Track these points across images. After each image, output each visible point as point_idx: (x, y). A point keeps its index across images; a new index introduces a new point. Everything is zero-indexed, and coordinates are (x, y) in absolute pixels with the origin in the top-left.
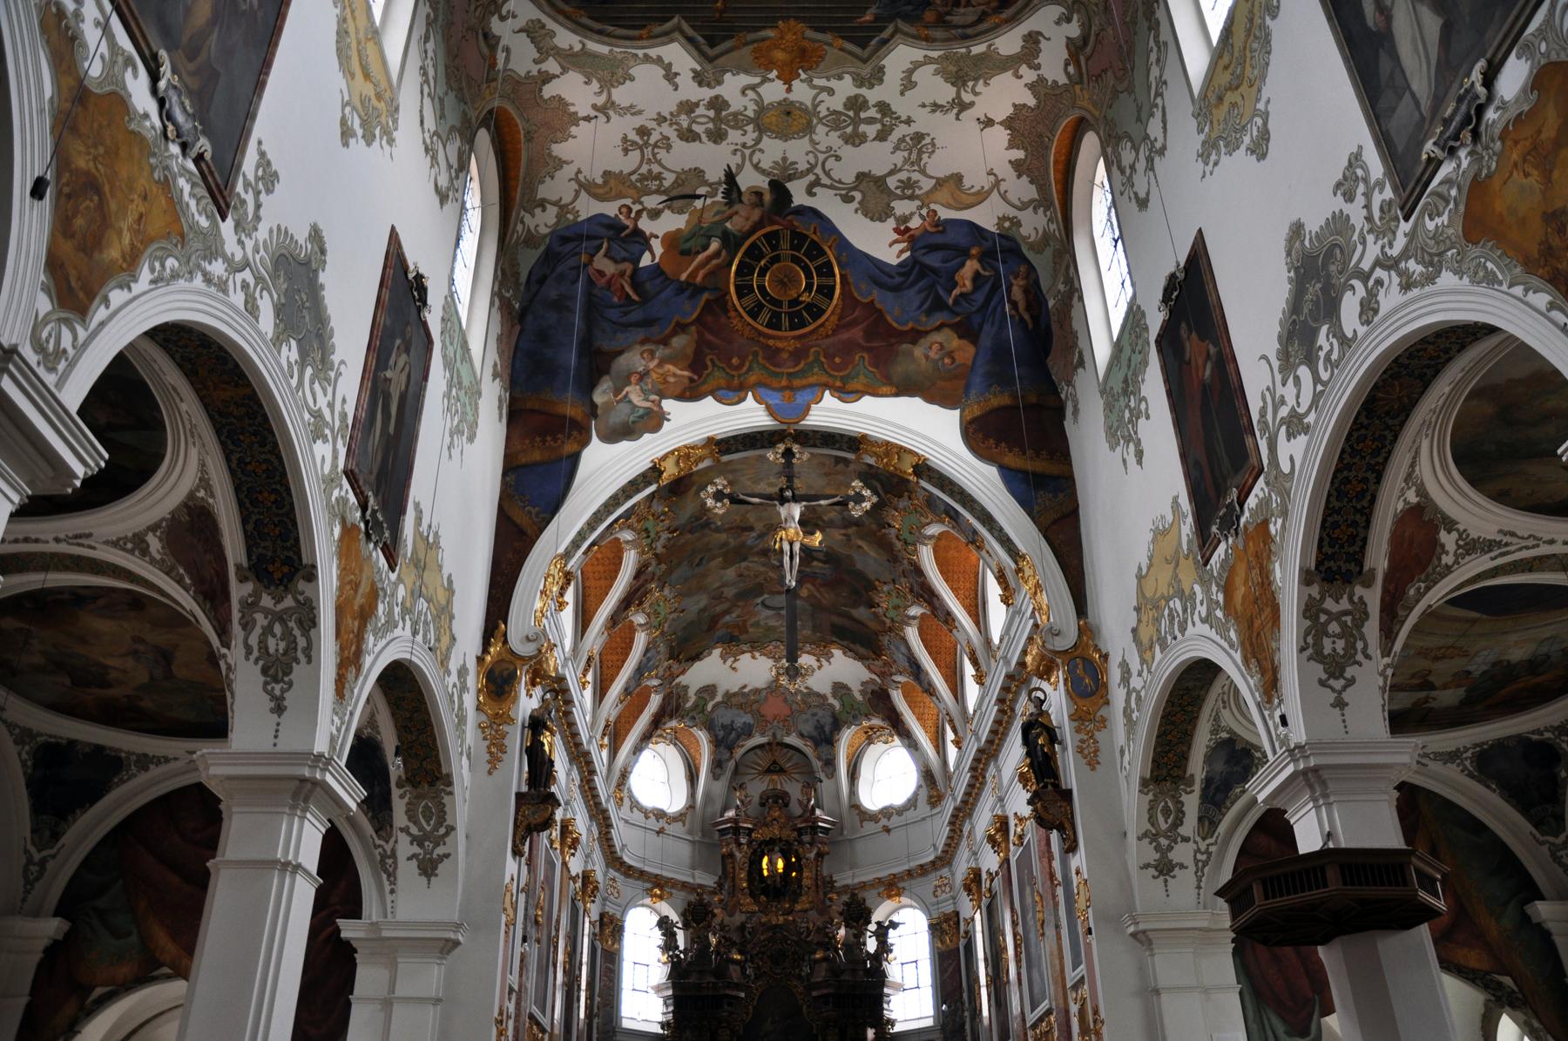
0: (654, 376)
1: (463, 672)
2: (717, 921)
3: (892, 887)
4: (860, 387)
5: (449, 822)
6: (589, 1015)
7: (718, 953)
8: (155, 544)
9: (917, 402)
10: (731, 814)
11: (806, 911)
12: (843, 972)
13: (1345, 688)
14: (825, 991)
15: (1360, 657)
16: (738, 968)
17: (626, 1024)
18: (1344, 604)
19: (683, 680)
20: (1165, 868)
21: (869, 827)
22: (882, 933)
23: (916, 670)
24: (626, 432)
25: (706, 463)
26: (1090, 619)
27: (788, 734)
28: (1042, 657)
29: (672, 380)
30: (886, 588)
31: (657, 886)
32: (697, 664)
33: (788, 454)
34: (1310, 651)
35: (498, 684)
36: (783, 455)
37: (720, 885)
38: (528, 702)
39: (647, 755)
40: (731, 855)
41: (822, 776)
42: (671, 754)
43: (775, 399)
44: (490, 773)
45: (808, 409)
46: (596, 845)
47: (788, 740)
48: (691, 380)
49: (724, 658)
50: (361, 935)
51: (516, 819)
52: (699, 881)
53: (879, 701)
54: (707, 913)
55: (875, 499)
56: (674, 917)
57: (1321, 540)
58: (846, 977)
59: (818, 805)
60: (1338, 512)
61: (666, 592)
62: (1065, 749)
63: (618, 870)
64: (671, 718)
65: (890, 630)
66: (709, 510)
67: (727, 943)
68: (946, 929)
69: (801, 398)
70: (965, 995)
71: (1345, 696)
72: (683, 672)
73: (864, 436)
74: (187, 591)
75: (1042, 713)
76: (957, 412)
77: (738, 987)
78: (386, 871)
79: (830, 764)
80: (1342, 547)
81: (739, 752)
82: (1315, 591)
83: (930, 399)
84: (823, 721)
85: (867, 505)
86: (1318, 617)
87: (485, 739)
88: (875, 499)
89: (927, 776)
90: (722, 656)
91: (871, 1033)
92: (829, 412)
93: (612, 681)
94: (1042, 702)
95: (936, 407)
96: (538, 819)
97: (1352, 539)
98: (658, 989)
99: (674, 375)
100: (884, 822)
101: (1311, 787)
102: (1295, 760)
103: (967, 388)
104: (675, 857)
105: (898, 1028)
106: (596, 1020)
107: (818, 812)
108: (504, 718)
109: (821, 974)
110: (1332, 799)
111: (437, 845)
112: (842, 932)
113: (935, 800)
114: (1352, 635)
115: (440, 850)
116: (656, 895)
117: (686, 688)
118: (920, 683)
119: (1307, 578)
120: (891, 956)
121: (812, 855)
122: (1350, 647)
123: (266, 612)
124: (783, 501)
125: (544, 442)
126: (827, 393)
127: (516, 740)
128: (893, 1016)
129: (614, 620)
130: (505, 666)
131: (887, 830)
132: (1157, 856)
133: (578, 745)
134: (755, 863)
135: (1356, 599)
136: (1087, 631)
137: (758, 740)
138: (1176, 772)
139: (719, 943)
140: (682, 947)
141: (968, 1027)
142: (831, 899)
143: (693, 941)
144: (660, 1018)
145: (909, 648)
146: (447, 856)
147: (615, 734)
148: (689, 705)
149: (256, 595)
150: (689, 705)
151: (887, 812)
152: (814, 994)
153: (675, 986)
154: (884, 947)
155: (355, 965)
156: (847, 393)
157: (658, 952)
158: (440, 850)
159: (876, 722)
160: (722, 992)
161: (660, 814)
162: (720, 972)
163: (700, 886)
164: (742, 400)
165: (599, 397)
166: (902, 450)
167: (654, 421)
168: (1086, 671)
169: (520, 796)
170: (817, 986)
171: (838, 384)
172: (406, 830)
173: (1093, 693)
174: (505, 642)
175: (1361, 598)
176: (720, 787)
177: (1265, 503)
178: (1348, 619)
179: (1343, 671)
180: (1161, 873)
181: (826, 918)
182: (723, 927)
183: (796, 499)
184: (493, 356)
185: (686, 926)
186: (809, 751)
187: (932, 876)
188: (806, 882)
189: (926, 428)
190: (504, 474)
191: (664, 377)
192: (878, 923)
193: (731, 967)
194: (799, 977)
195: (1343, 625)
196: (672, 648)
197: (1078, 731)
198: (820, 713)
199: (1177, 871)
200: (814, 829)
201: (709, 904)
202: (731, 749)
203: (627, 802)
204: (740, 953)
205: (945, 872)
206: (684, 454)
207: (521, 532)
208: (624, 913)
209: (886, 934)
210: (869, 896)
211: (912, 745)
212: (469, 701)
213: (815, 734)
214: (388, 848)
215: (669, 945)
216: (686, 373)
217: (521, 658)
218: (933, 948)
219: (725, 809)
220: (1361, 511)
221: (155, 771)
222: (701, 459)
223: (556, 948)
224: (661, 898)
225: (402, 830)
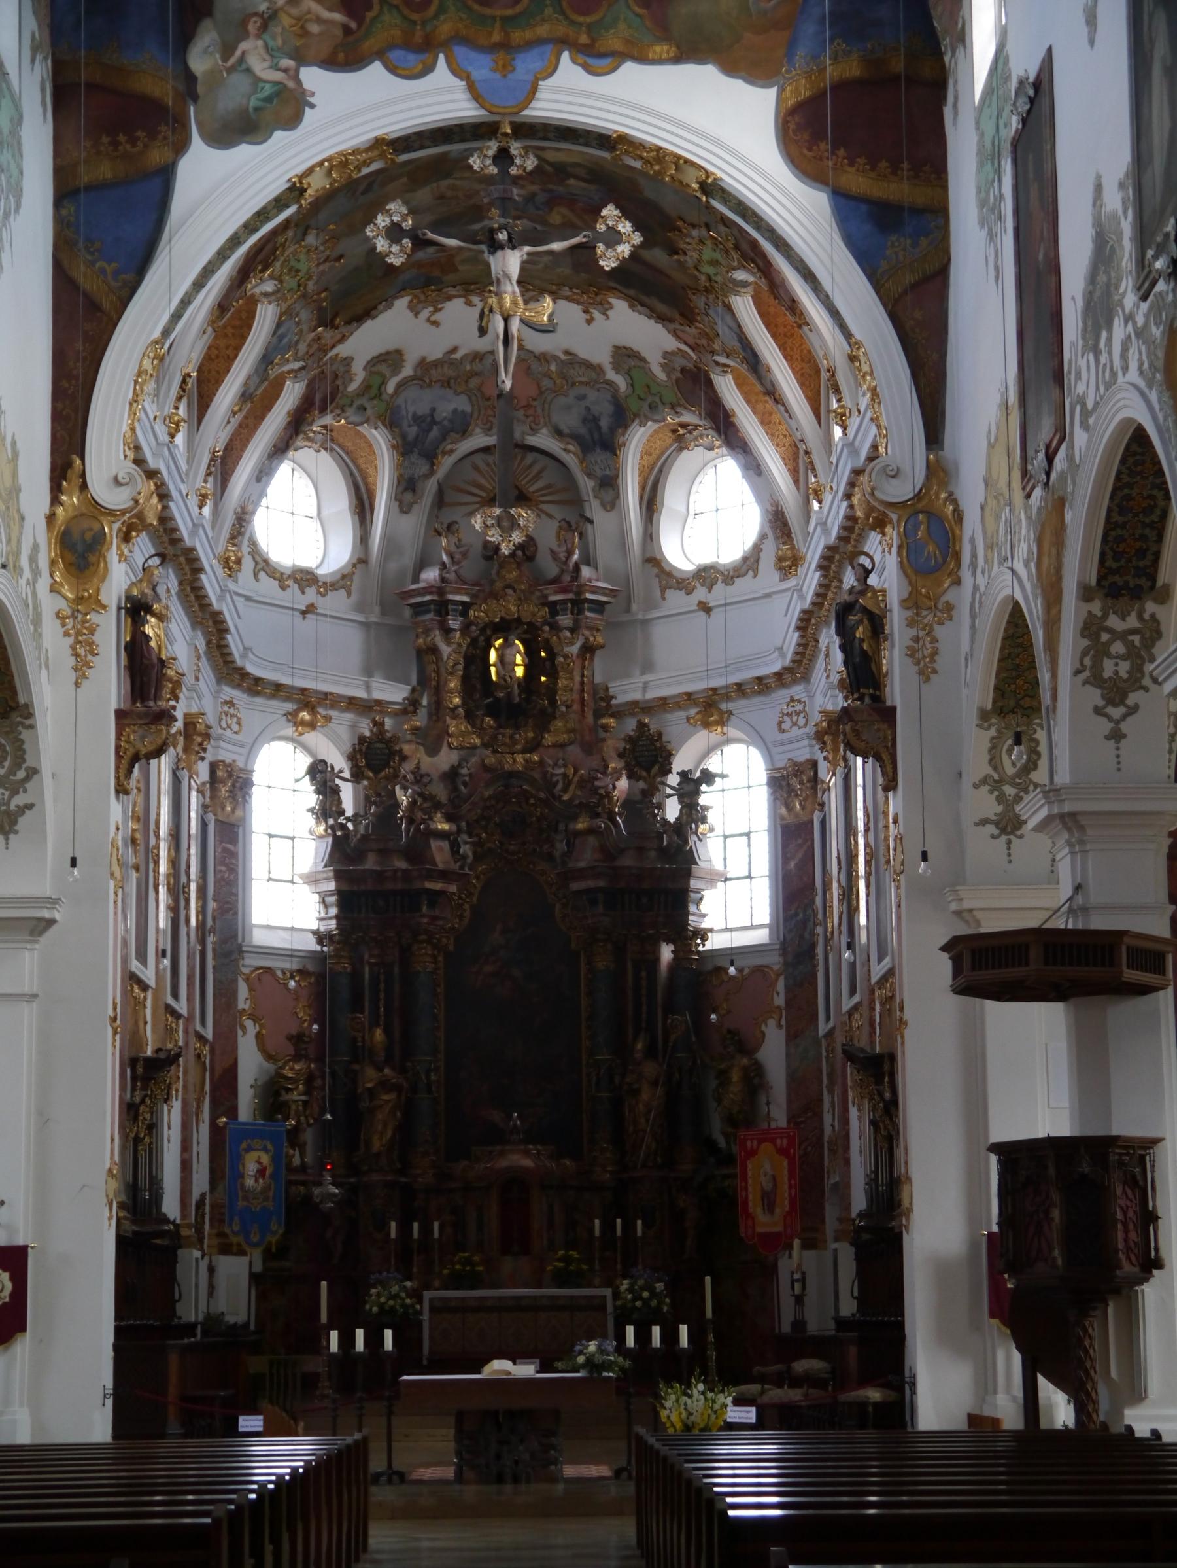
0: (286, 21)
1: (33, 560)
2: (407, 768)
3: (711, 708)
4: (617, 45)
5: (30, 762)
6: (201, 925)
7: (411, 821)
9: (709, 72)
10: (431, 575)
11: (562, 746)
12: (622, 851)
13: (1124, 717)
14: (591, 884)
15: (1147, 681)
16: (445, 845)
17: (260, 938)
18: (1132, 622)
19: (342, 350)
20: (1009, 825)
21: (676, 600)
22: (691, 787)
23: (753, 361)
24: (243, 127)
25: (375, 166)
26: (948, 451)
27: (534, 431)
28: (870, 509)
29: (314, 28)
30: (695, 233)
31: (306, 707)
32: (369, 325)
33: (503, 157)
34: (1087, 674)
35: (79, 551)
37: (412, 704)
38: (118, 578)
39: (285, 469)
40: (434, 650)
41: (594, 509)
42: (326, 464)
43: (482, 67)
44: (77, 685)
45: (534, 90)
46: (205, 665)
47: (532, 440)
48: (347, 30)
49: (414, 310)
51: (118, 747)
52: (377, 695)
53: (694, 386)
54: (392, 753)
55: (637, 239)
56: (338, 761)
57: (1103, 555)
58: (627, 861)
59: (588, 560)
60: (1123, 526)
61: (311, 239)
62: (893, 646)
63: (238, 686)
64: (323, 411)
65: (707, 290)
66: (382, 257)
67: (425, 803)
68: (793, 786)
69: (526, 64)
70: (818, 900)
71: (1124, 727)
72: (343, 339)
73: (623, 139)
75: (865, 589)
76: (771, 93)
77: (444, 875)
79: (610, 484)
80: (1129, 560)
81: (446, 464)
82: (1096, 607)
83: (731, 68)
84: (596, 410)
85: (624, 250)
86: (1098, 637)
87: (67, 634)
88: (637, 239)
89: (778, 523)
90: (411, 307)
91: (667, 953)
92: (571, 93)
93: (219, 382)
94: (868, 572)
95: (738, 87)
96: (148, 745)
97: (1141, 553)
98: (311, 879)
99: (319, 20)
100: (700, 594)
101: (1069, 830)
102: (1050, 803)
103: (792, 45)
104: (336, 656)
105: (714, 942)
106: (211, 939)
107: (586, 572)
108: (85, 604)
109: (586, 857)
110: (1088, 847)
111: (15, 792)
112: (623, 784)
113: (789, 564)
114: (1140, 657)
115: (19, 800)
116: (303, 723)
117: (348, 361)
118: (760, 378)
119: (1086, 594)
120: (702, 828)
121: (574, 649)
122: (1137, 670)
124: (495, 246)
125: (115, 144)
126: (565, 56)
127: (109, 632)
128: (705, 924)
129: (222, 307)
130: (86, 524)
131: (705, 608)
132: (999, 809)
133: (176, 541)
134: (476, 660)
135: (1146, 616)
136: (939, 473)
137: (479, 439)
138: (1027, 702)
139: (413, 804)
140: (349, 813)
141: (820, 950)
142: (605, 728)
143: (368, 801)
144: (314, 925)
145: (739, 326)
146: (30, 807)
147: (223, 466)
148: (353, 387)
150: (353, 387)
151: (707, 575)
152: (575, 886)
153: (339, 876)
154: (693, 813)
156: (598, 56)
157: (310, 820)
158: (19, 800)
159: (688, 417)
160: (417, 885)
161: (305, 578)
162: (416, 852)
163: (379, 702)
164: (428, 69)
165: (200, 60)
166: (680, 163)
167: (288, 108)
168: (932, 534)
169: (120, 714)
170: (580, 874)
171: (584, 39)
173: (937, 568)
174: (84, 487)
175: (1153, 616)
176: (412, 525)
177: (1062, 476)
178: (1136, 639)
179: (1124, 696)
180: (1003, 831)
181: (595, 762)
182: (419, 777)
183: (513, 244)
184: (31, 24)
185: (357, 776)
186: (571, 460)
188: (561, 697)
189: (722, 125)
190: (58, 202)
191: (301, 22)
192: (684, 775)
193: (434, 844)
194: (550, 857)
195: (1130, 645)
196: (320, 309)
197: (911, 623)
198: (592, 395)
200: (578, 604)
201: (394, 739)
202: (431, 457)
203: (248, 564)
204: (449, 818)
205: (797, 691)
206: (340, 162)
207: (93, 306)
208: (252, 750)
209: (697, 792)
210: (673, 724)
211: (754, 468)
212: (44, 583)
213: (583, 431)
215: (329, 807)
216: (337, 17)
217: (111, 513)
218: (774, 815)
219: (422, 564)
220: (1151, 525)
222: (366, 163)
223: (157, 863)
224: (312, 726)
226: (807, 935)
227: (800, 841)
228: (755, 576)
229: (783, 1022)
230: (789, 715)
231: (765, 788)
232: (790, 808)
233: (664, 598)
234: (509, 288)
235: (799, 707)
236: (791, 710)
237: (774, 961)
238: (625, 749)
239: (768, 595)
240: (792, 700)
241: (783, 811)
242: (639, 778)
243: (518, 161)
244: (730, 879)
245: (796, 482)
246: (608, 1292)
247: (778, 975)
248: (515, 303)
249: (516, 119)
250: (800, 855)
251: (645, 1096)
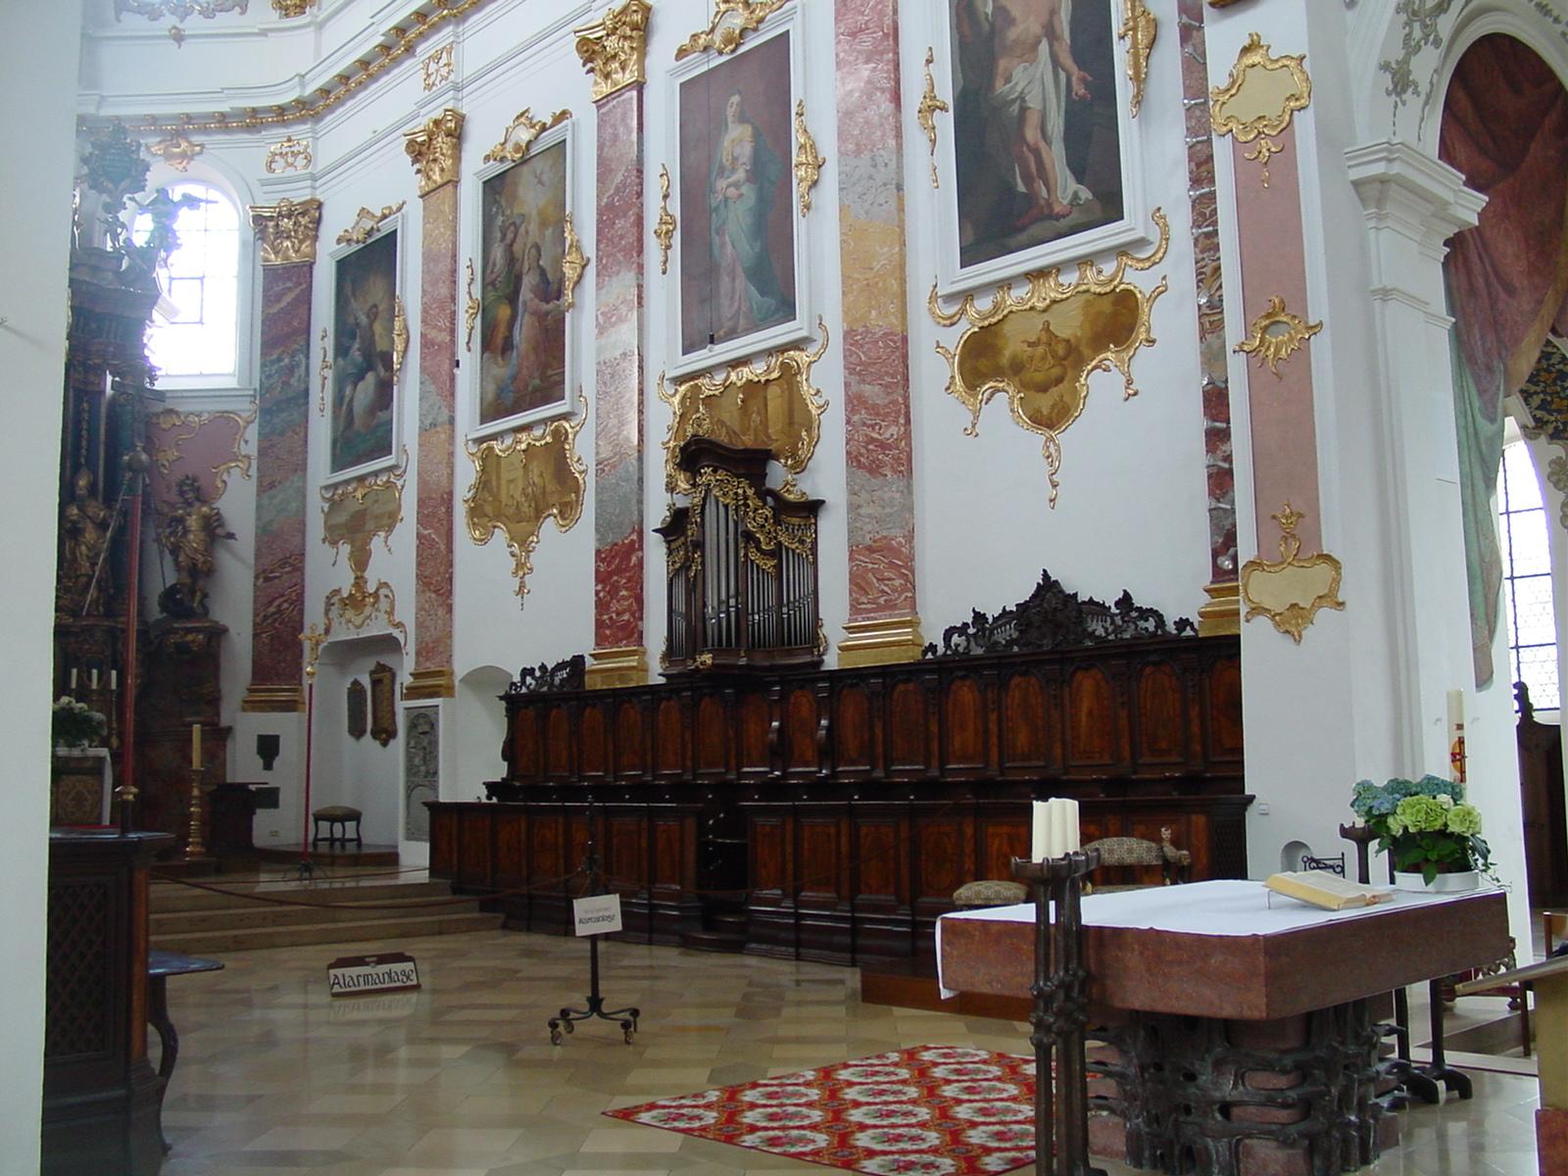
131: (179, 37)
154: (165, 238)
187: (273, 139)
199: (1408, 96)
205: (301, 131)
226: (293, 381)
227: (289, 284)
228: (243, 12)
229: (253, 471)
231: (237, 233)
233: (118, 20)
236: (284, 151)
237: (246, 408)
238: (91, 154)
240: (289, 140)
242: (101, 190)
244: (201, 319)
246: (104, 752)
247: (249, 423)
250: (288, 298)
251: (90, 535)
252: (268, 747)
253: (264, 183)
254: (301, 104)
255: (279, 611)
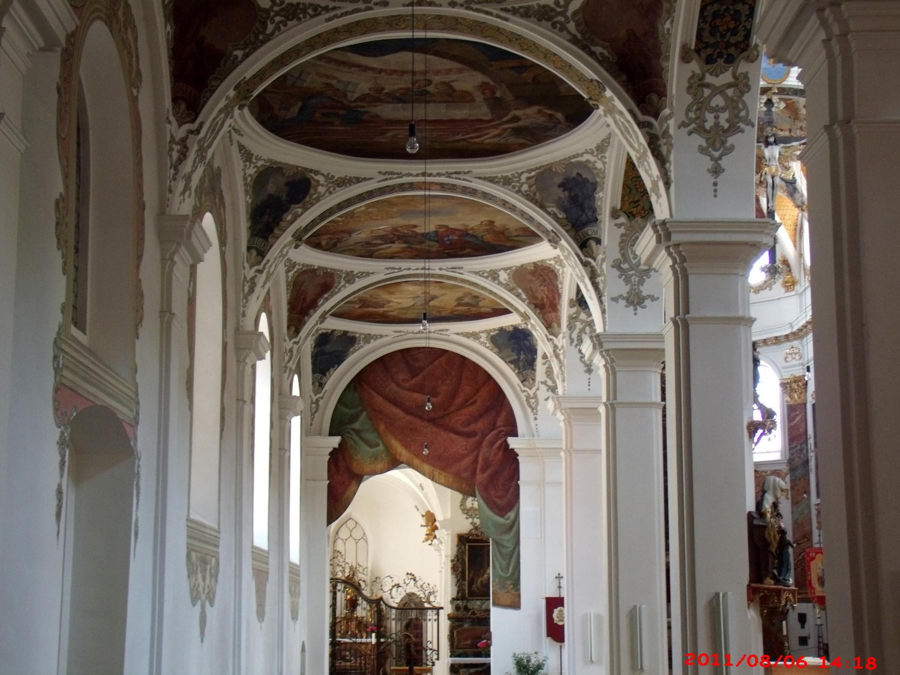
8: (503, 276)
33: (769, 103)
36: (766, 104)
50: (523, 446)
74: (523, 301)
78: (530, 406)
123: (582, 322)
149: (578, 313)
155: (517, 463)
172: (544, 383)
183: (776, 143)
187: (786, 348)
205: (796, 343)
214: (531, 392)
221: (374, 344)
225: (542, 383)
229: (789, 496)
230: (791, 354)
232: (791, 397)
234: (774, 163)
235: (797, 351)
239: (778, 299)
241: (788, 399)
243: (776, 105)
245: (795, 246)
248: (777, 170)
249: (779, 86)
252: (802, 618)
253: (785, 368)
254: (793, 334)
255: (803, 558)
